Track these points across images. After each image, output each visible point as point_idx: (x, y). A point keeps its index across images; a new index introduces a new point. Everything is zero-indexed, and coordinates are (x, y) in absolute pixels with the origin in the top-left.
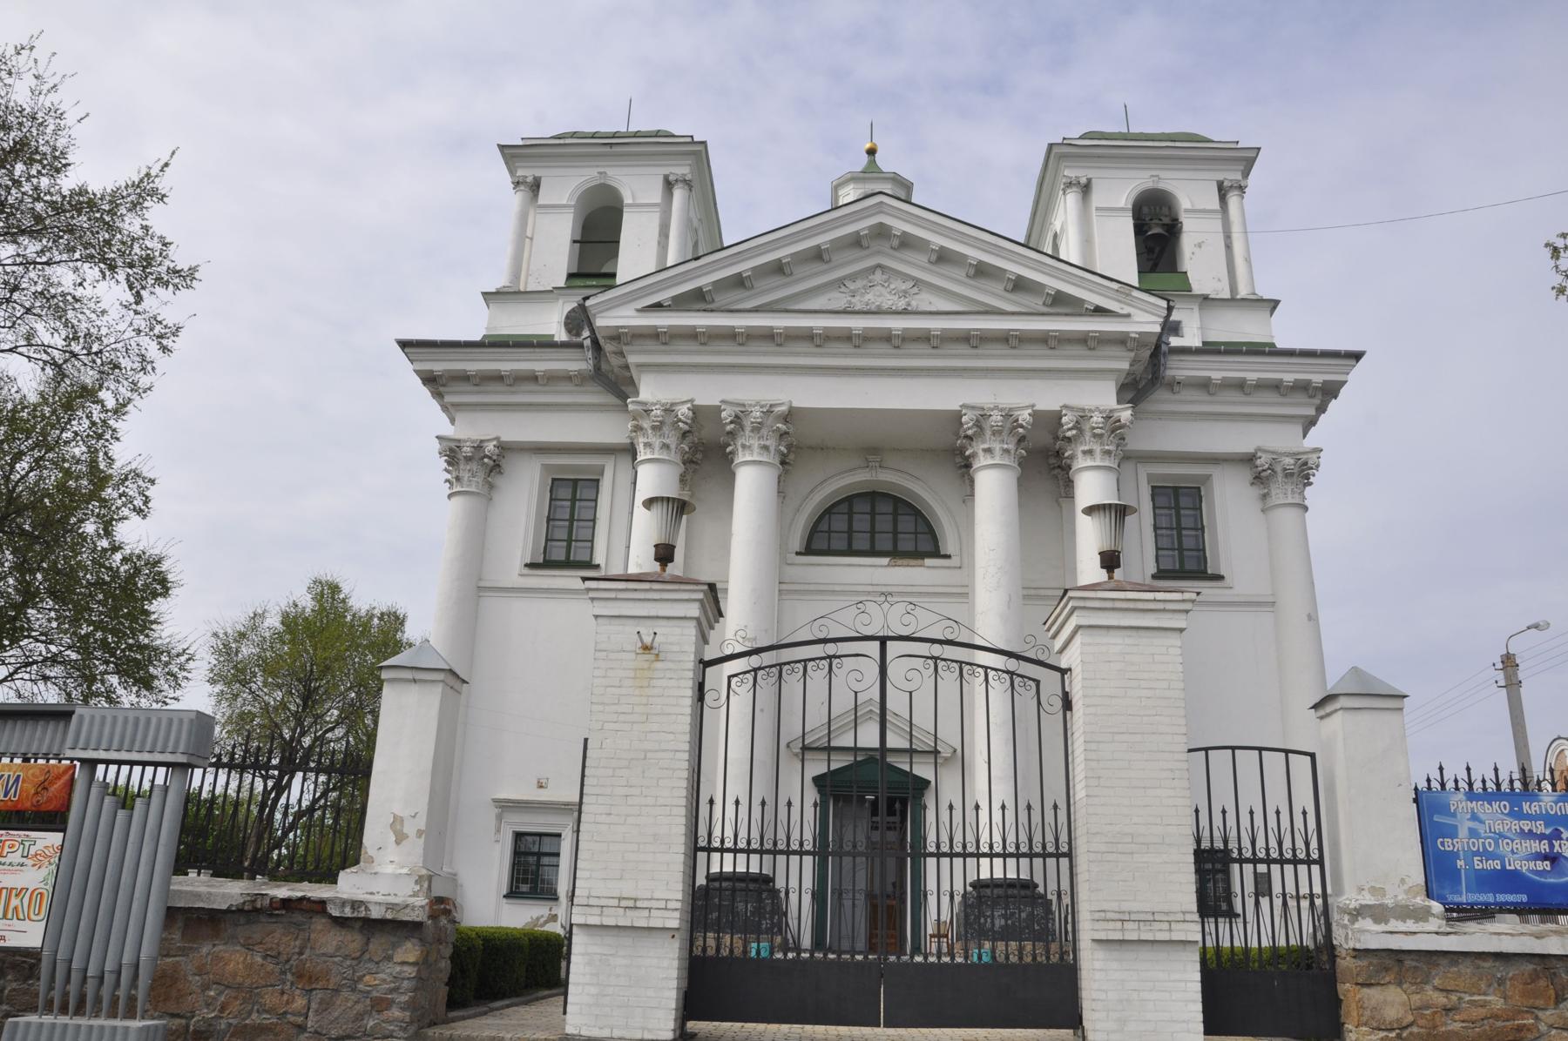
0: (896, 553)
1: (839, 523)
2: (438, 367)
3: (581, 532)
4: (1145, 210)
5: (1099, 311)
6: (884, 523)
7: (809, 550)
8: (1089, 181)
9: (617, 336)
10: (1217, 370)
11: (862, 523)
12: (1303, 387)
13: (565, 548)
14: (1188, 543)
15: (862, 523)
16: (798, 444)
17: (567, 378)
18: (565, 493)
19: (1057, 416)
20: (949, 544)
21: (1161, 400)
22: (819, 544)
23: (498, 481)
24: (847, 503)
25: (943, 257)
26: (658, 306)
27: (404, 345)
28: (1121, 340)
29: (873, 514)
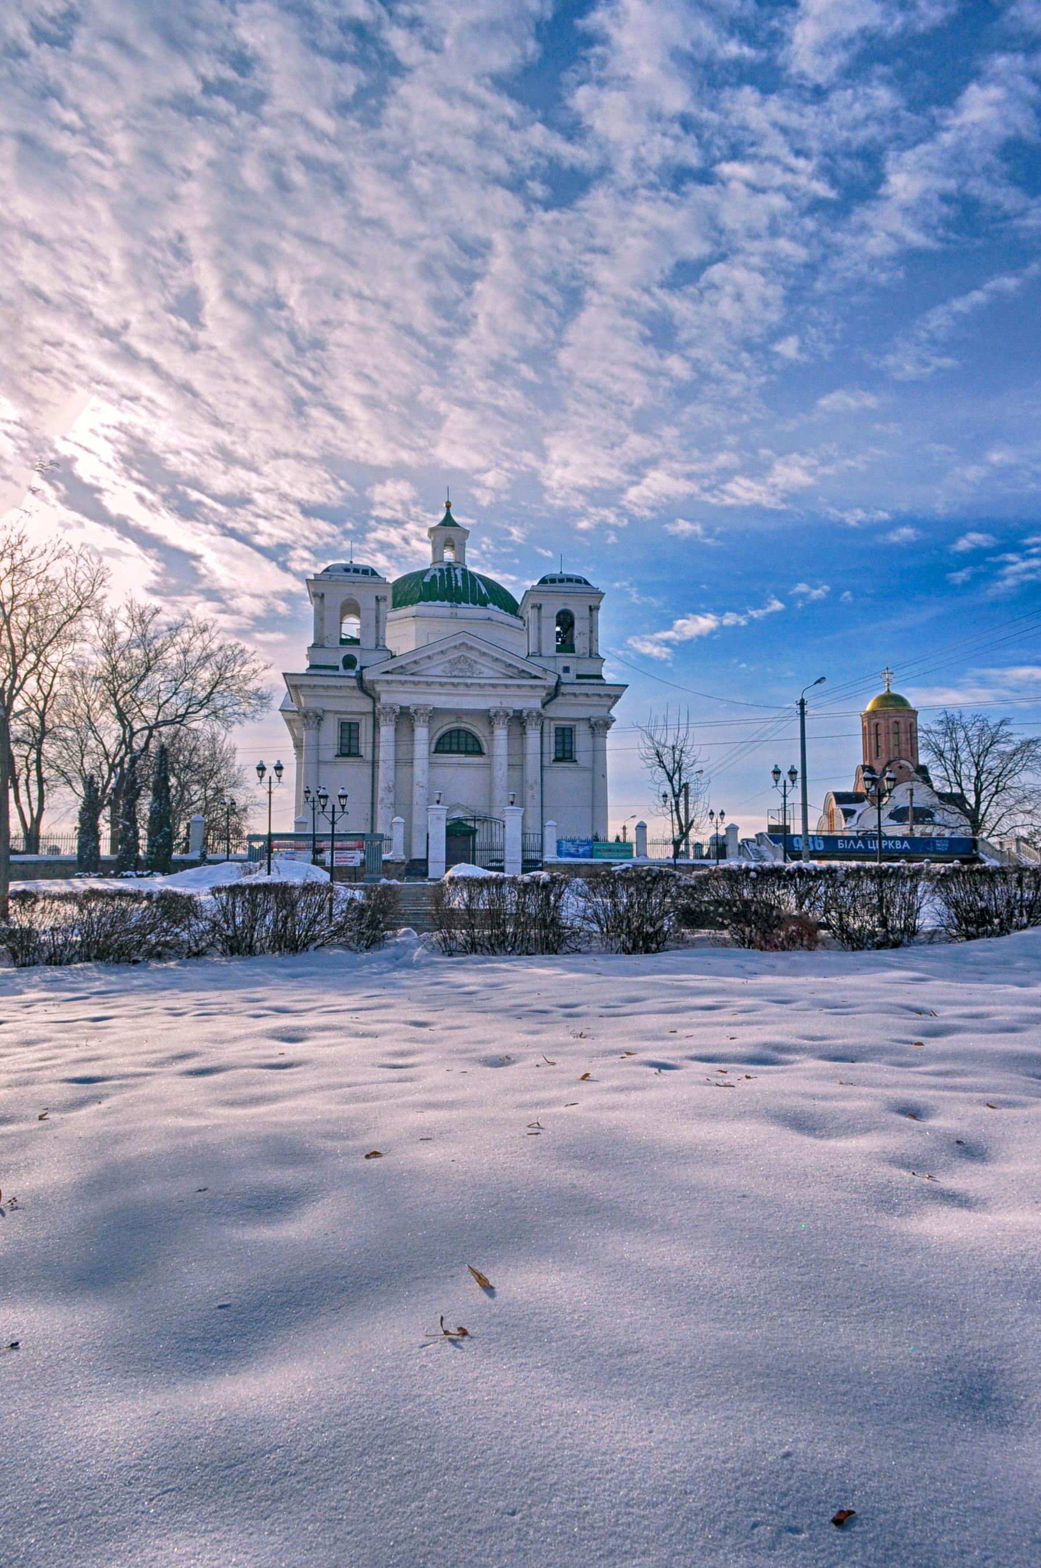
0: (467, 752)
1: (447, 740)
2: (298, 683)
3: (353, 742)
5: (536, 677)
6: (462, 740)
7: (436, 751)
9: (373, 682)
10: (576, 689)
11: (454, 740)
12: (609, 696)
13: (348, 749)
14: (567, 748)
15: (454, 740)
18: (346, 727)
19: (521, 711)
20: (485, 751)
21: (559, 699)
22: (441, 748)
24: (450, 733)
25: (484, 654)
26: (387, 672)
27: (284, 674)
28: (544, 687)
29: (459, 737)
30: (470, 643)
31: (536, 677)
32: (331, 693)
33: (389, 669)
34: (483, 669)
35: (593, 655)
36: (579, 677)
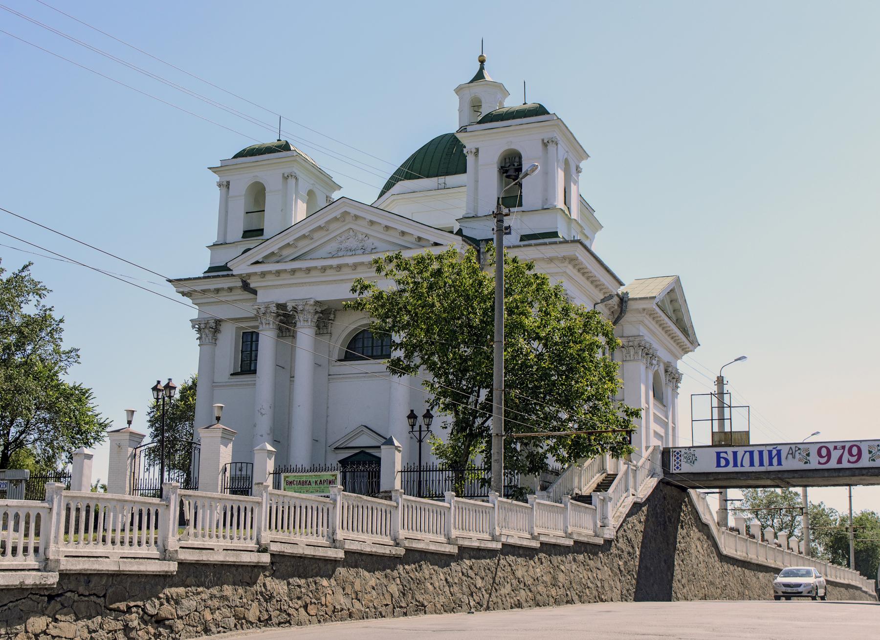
4: (507, 160)
5: (436, 244)
8: (477, 150)
16: (325, 315)
17: (236, 287)
23: (219, 336)
26: (257, 263)
30: (354, 212)
31: (436, 244)
32: (223, 296)
33: (259, 258)
34: (377, 244)
35: (547, 208)
36: (524, 238)
